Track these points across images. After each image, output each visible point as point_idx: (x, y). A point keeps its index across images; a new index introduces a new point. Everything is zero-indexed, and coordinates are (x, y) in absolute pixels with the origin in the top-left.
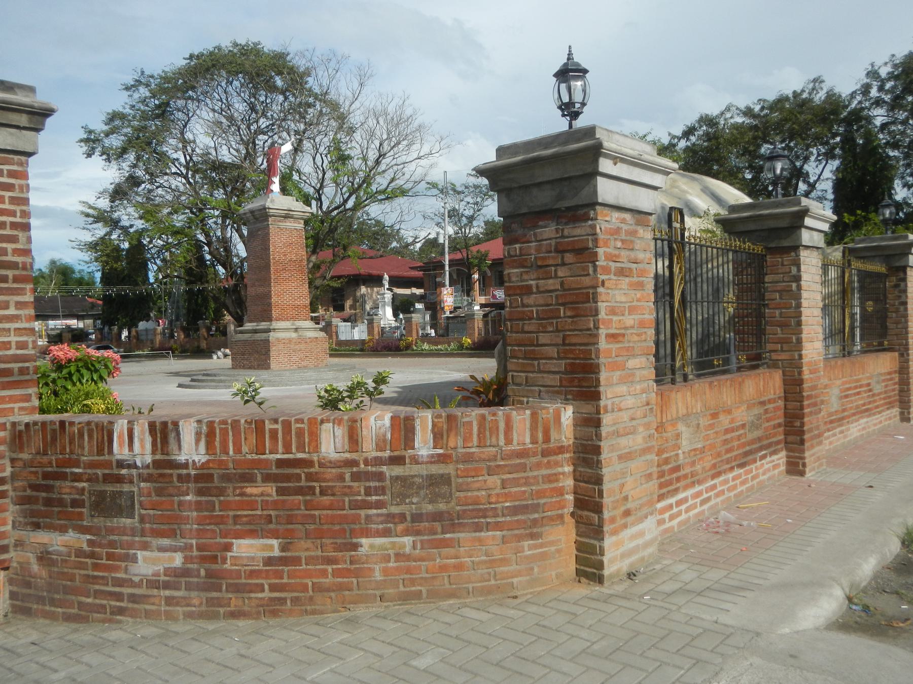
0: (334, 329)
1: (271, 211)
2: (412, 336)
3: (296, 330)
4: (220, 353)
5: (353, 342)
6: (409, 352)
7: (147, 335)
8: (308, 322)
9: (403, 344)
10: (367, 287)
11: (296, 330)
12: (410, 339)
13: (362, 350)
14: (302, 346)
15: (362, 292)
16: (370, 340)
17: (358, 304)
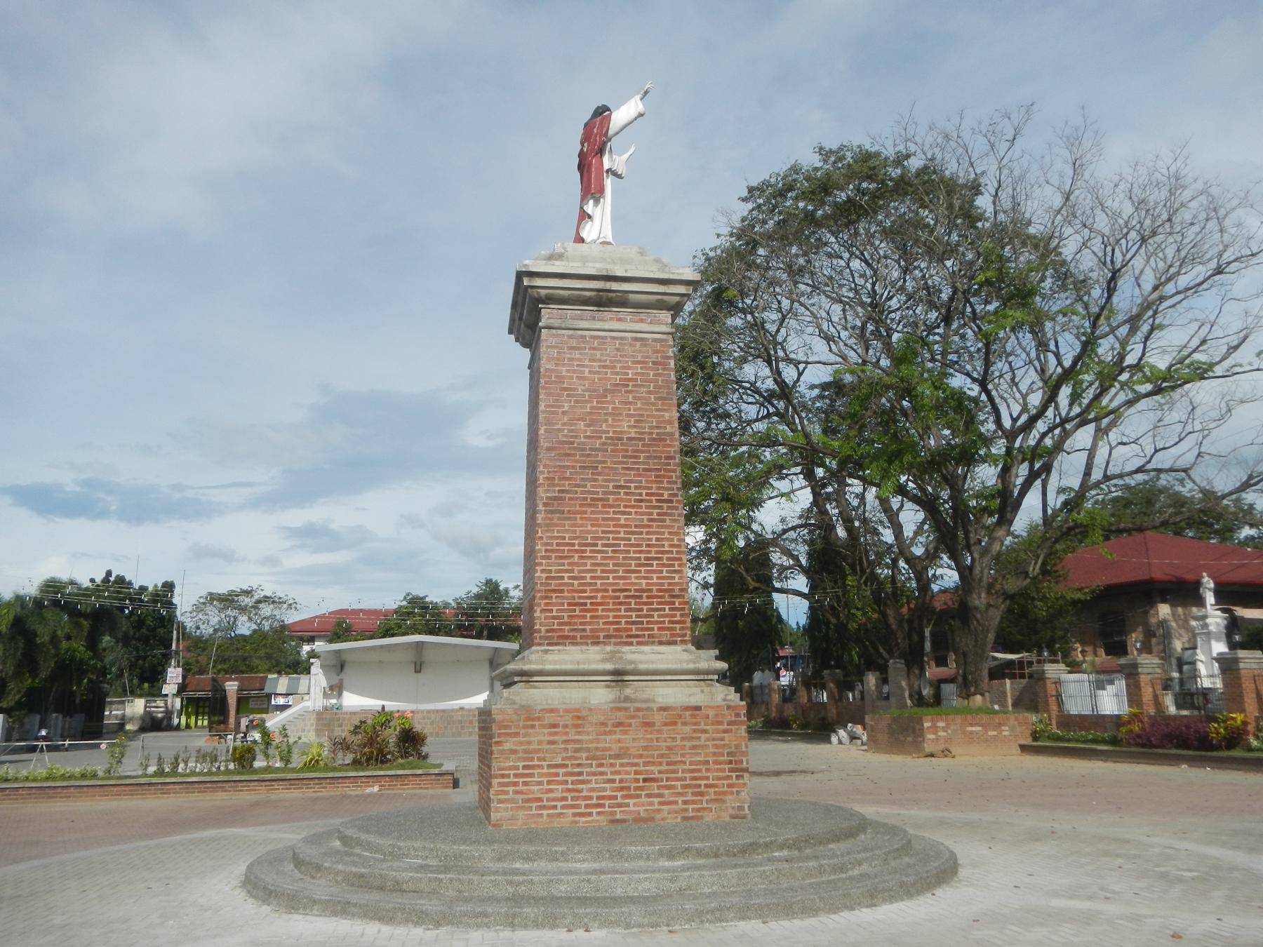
0: (1051, 688)
1: (539, 282)
2: (1242, 711)
3: (619, 677)
4: (842, 733)
5: (1096, 721)
6: (1237, 753)
7: (762, 693)
8: (678, 648)
9: (1216, 730)
10: (1173, 605)
11: (619, 677)
12: (1239, 717)
13: (1114, 741)
14: (633, 739)
15: (1161, 616)
16: (1134, 717)
17: (1154, 640)
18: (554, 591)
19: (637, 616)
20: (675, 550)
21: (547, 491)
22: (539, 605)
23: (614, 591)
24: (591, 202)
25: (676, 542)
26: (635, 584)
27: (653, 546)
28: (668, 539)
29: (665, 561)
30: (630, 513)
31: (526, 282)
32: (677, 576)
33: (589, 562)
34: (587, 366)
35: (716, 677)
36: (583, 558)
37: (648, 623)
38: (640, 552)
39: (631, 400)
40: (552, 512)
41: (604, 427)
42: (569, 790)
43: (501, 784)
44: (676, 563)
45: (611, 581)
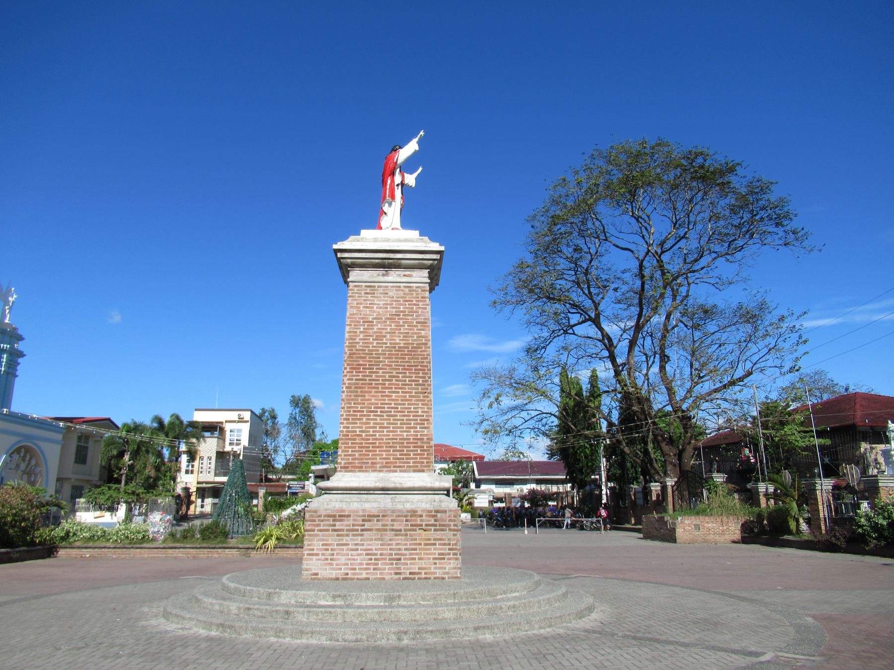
1: (346, 255)
18: (351, 439)
19: (400, 455)
20: (425, 414)
21: (349, 379)
22: (341, 447)
23: (386, 439)
24: (387, 205)
25: (426, 410)
26: (400, 435)
27: (411, 412)
28: (421, 408)
29: (419, 421)
30: (398, 392)
31: (339, 255)
32: (426, 430)
33: (372, 422)
34: (376, 304)
35: (446, 492)
36: (368, 419)
37: (407, 459)
38: (404, 416)
39: (401, 324)
40: (351, 392)
41: (384, 341)
42: (349, 559)
43: (308, 555)
44: (426, 422)
45: (385, 433)
